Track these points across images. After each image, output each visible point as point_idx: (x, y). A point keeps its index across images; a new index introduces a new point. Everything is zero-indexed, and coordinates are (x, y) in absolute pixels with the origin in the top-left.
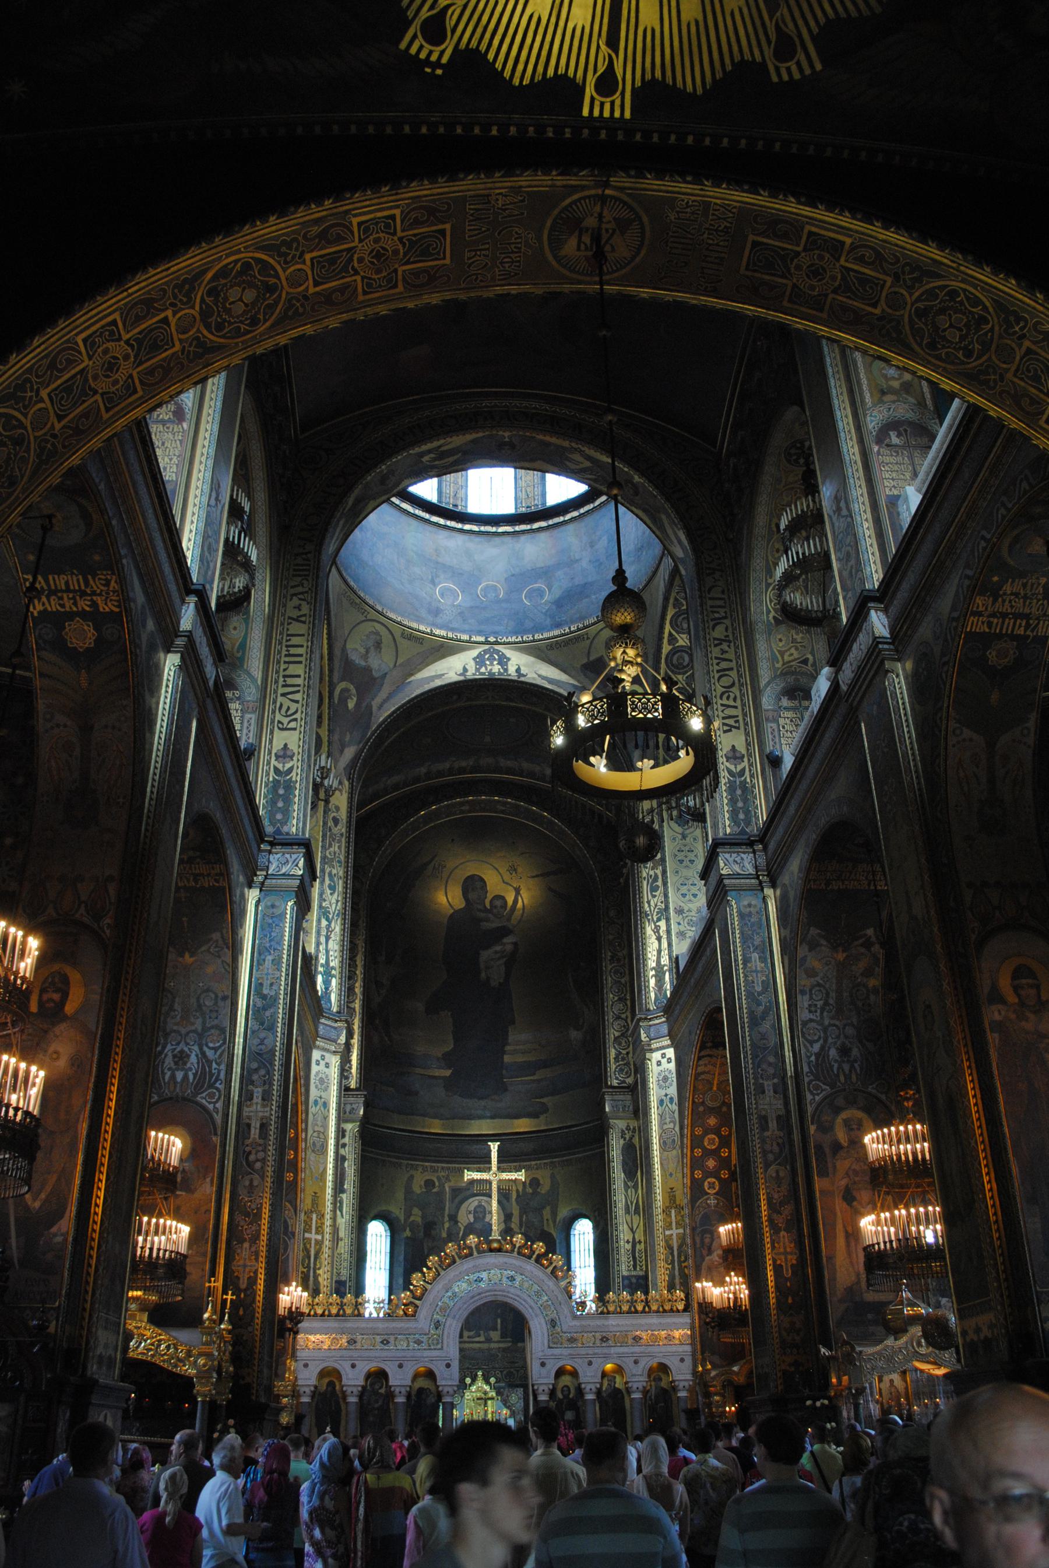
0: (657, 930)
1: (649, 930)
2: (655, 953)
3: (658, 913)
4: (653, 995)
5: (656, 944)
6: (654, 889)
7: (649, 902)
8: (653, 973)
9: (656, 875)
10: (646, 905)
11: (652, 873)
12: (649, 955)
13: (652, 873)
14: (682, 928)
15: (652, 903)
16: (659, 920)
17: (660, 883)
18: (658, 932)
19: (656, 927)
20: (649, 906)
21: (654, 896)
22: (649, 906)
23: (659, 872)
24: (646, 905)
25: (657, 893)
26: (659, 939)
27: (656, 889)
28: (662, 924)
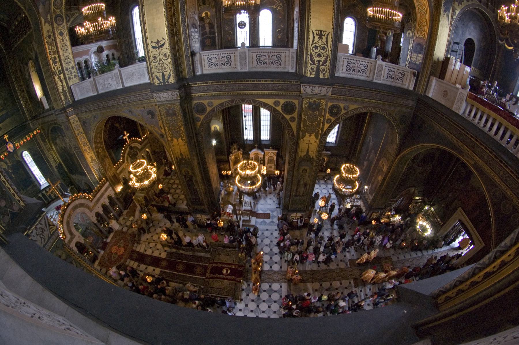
0: (60, 78)
1: (56, 79)
2: (61, 87)
3: (59, 72)
4: (64, 102)
5: (61, 84)
6: (55, 63)
7: (54, 68)
8: (62, 94)
9: (55, 57)
10: (53, 69)
11: (53, 56)
12: (59, 88)
13: (53, 56)
14: (69, 76)
15: (56, 68)
16: (60, 74)
17: (57, 60)
18: (60, 79)
19: (59, 77)
20: (55, 69)
21: (56, 66)
22: (55, 69)
23: (57, 56)
24: (53, 69)
25: (57, 64)
26: (61, 81)
27: (56, 62)
28: (62, 76)
